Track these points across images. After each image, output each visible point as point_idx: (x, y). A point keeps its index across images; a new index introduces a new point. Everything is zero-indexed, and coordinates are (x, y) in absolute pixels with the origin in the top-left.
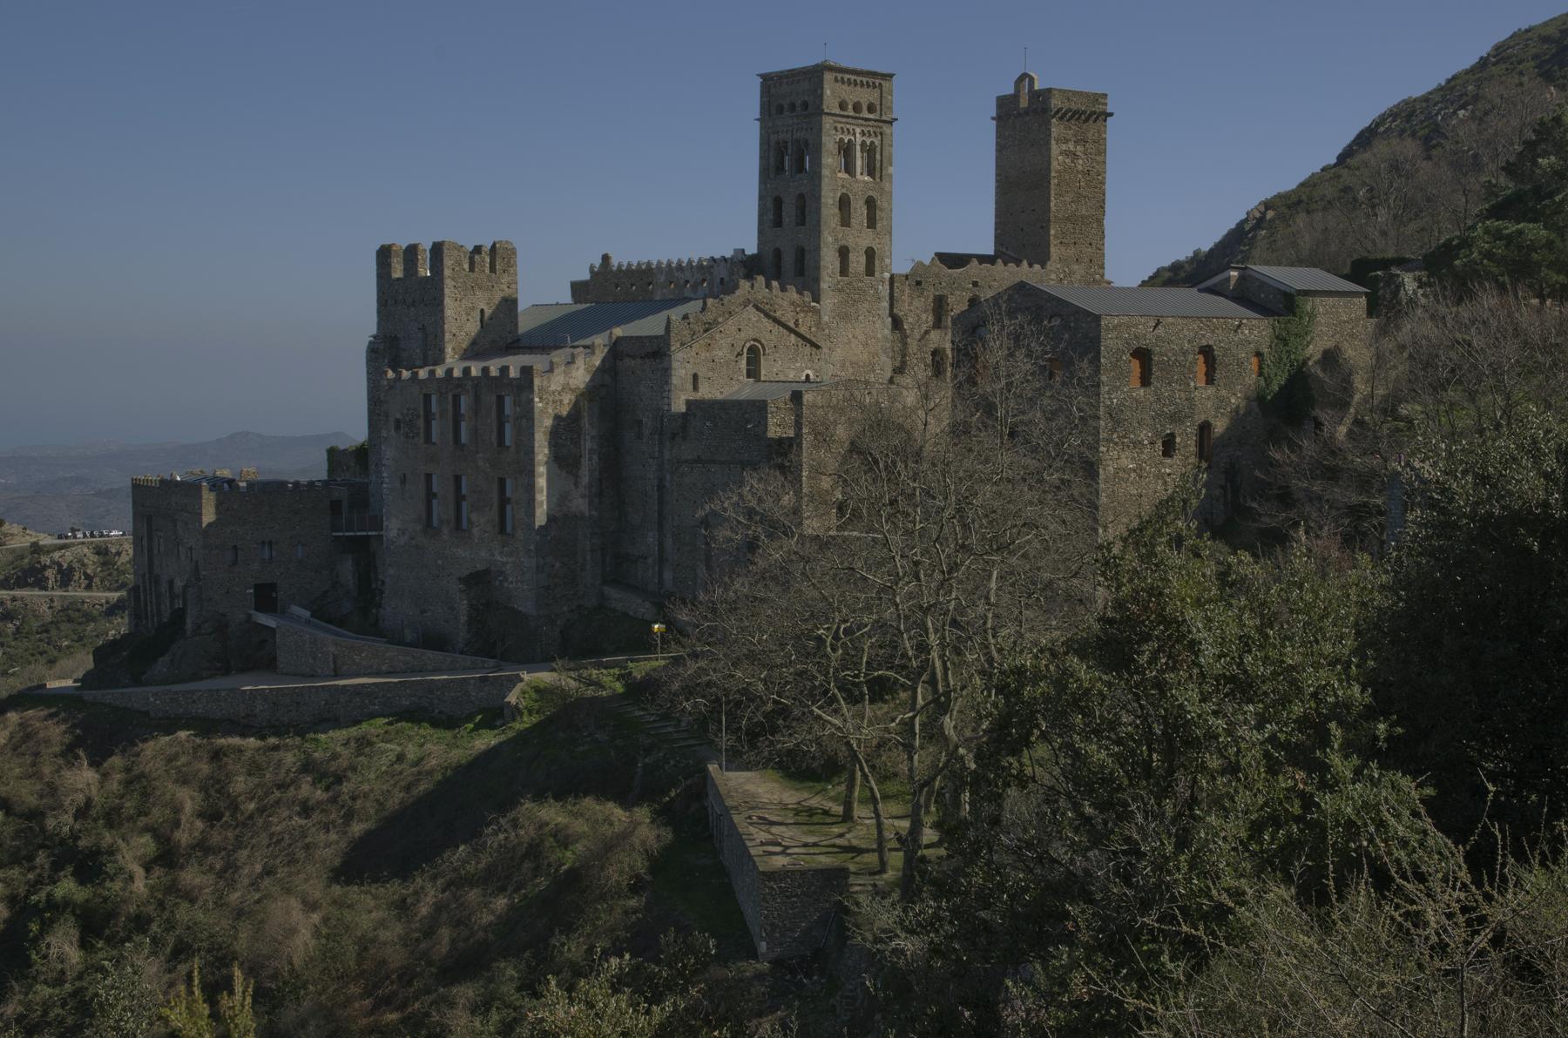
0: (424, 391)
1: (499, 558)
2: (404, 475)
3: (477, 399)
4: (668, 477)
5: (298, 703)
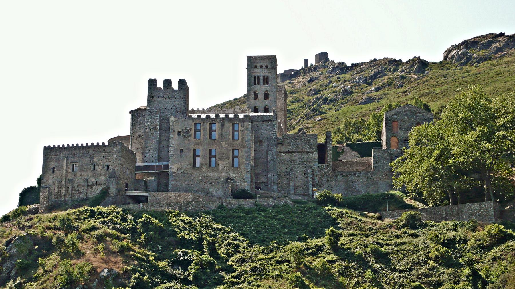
0: (195, 122)
1: (232, 175)
2: (181, 150)
3: (223, 125)
4: (275, 157)
5: (205, 207)
